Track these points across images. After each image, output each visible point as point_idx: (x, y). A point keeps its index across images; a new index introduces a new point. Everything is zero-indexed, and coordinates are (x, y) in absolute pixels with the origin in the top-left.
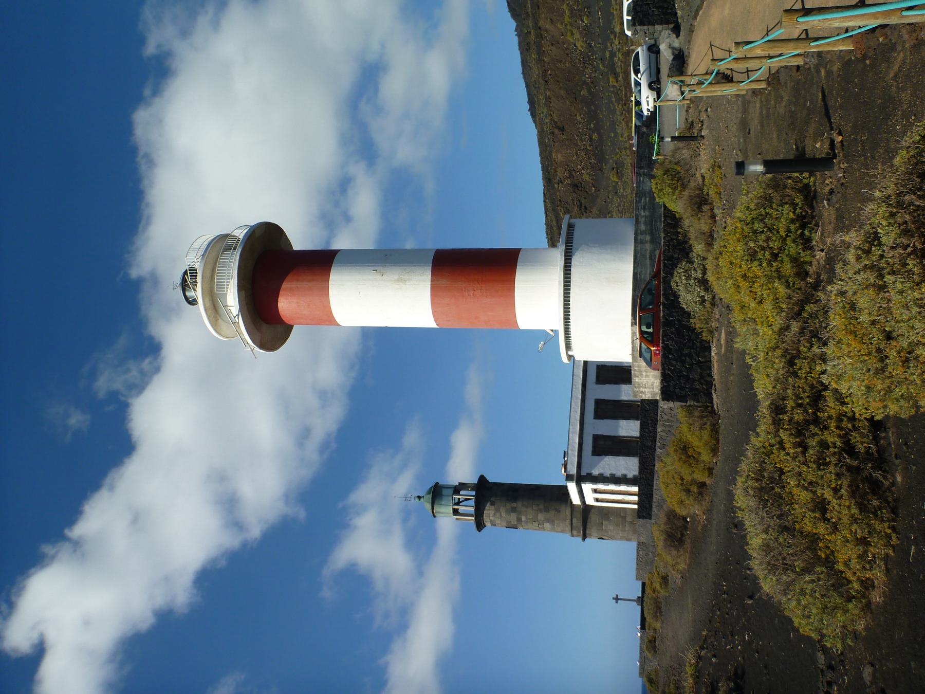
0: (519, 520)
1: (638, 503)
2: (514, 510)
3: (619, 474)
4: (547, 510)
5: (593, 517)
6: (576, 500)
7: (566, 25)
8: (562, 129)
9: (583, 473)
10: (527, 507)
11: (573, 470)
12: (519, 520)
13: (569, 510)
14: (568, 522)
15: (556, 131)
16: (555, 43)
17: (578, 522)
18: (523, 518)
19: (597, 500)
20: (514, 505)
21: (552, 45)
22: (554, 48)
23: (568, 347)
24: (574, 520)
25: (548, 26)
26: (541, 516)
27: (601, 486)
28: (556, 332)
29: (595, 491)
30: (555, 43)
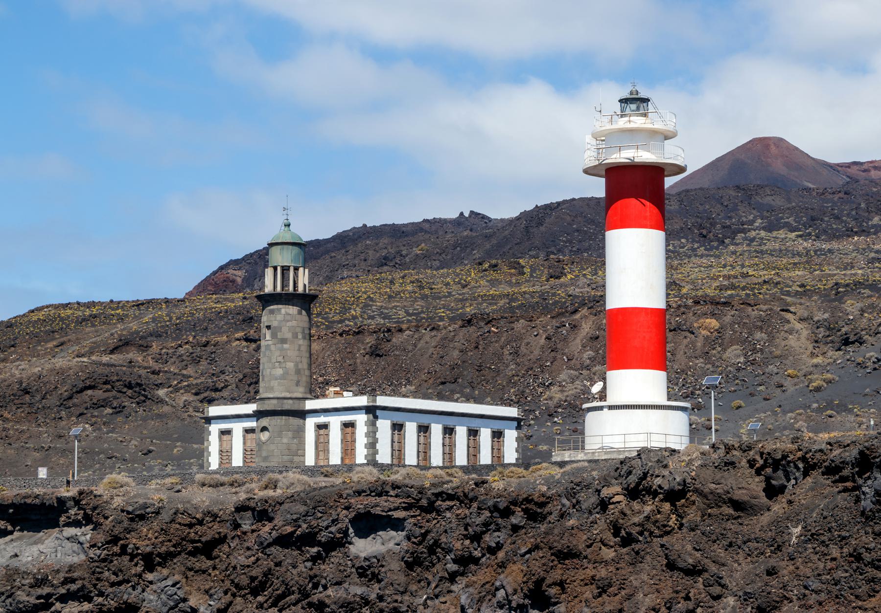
0: (284, 341)
2: (295, 336)
3: (378, 446)
4: (298, 372)
5: (294, 421)
7: (588, 368)
8: (375, 353)
9: (378, 412)
10: (299, 350)
11: (382, 401)
12: (284, 341)
13: (300, 396)
14: (288, 395)
15: (370, 340)
16: (553, 345)
17: (288, 405)
18: (285, 346)
20: (300, 336)
21: (548, 338)
22: (542, 341)
23: (611, 408)
24: (290, 401)
26: (290, 365)
28: (602, 395)
30: (553, 345)
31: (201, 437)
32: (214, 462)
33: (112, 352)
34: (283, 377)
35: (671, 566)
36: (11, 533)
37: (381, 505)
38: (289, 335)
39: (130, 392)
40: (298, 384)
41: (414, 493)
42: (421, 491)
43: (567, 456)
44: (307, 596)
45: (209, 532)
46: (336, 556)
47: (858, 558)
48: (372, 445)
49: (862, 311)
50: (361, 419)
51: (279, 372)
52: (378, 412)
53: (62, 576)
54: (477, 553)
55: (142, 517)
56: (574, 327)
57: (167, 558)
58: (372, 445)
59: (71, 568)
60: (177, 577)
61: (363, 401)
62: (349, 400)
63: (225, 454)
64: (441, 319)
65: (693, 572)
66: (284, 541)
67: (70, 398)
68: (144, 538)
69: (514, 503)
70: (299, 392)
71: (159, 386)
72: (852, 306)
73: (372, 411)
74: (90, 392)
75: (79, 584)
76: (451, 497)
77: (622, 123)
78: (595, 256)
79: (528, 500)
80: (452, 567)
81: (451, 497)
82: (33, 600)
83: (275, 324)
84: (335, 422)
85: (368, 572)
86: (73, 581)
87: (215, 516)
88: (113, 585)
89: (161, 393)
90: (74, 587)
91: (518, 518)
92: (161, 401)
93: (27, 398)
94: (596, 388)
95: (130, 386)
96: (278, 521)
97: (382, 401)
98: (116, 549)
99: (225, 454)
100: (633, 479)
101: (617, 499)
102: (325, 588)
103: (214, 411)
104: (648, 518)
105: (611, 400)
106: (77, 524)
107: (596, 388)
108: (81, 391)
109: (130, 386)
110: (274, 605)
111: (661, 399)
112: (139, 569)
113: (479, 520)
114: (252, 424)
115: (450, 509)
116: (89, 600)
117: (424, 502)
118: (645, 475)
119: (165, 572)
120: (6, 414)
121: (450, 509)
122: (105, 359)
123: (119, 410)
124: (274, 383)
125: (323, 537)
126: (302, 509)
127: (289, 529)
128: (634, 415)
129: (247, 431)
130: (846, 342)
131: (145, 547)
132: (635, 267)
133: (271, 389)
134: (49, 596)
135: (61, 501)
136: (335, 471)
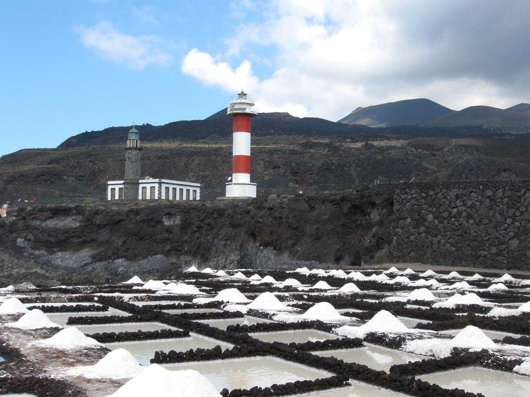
0: (133, 162)
1: (143, 200)
2: (136, 160)
4: (137, 171)
6: (140, 181)
7: (197, 173)
9: (162, 184)
12: (133, 162)
17: (134, 181)
19: (144, 188)
21: (185, 164)
25: (196, 161)
26: (135, 169)
27: (157, 189)
28: (231, 181)
29: (153, 188)
31: (106, 189)
32: (109, 198)
33: (48, 164)
34: (133, 172)
35: (290, 226)
36: (54, 218)
37: (173, 211)
38: (134, 160)
39: (55, 177)
40: (137, 175)
41: (183, 208)
42: (185, 207)
43: (221, 198)
44: (151, 237)
45: (117, 218)
46: (159, 226)
47: (344, 225)
48: (160, 194)
49: (279, 158)
50: (157, 186)
51: (131, 171)
52: (162, 184)
53: (72, 231)
54: (202, 225)
55: (97, 213)
56: (193, 161)
57: (105, 226)
58: (160, 194)
59: (75, 228)
60: (108, 231)
61: (157, 180)
62: (151, 180)
63: (113, 195)
64: (151, 157)
65: (296, 229)
66: (143, 221)
67: (36, 178)
68: (98, 220)
69: (215, 211)
70: (137, 177)
71: (64, 175)
72: (276, 157)
73: (160, 183)
74: (42, 177)
75: (78, 233)
76: (195, 209)
77: (239, 101)
78: (230, 140)
79: (219, 210)
80: (195, 229)
81: (195, 209)
82: (63, 238)
83: (130, 157)
84: (148, 186)
85: (169, 230)
86: (76, 232)
87: (120, 213)
88: (88, 233)
89: (65, 177)
90: (76, 234)
91: (215, 215)
92: (65, 180)
93: (23, 178)
94: (229, 179)
95: (55, 175)
96: (142, 215)
97: (163, 180)
98: (89, 223)
99: (113, 195)
100: (258, 204)
101: (253, 210)
102: (157, 234)
103: (109, 182)
104: (263, 215)
105: (234, 182)
106: (76, 215)
107: (229, 179)
108: (39, 176)
109: (55, 175)
110: (141, 239)
111: (249, 182)
112: (97, 229)
113: (204, 216)
114: (122, 186)
115: (193, 212)
116: (81, 238)
117: (186, 210)
118: (262, 203)
119: (104, 230)
120: (16, 183)
121: (193, 212)
122: (46, 166)
123: (52, 182)
124: (130, 175)
125: (156, 220)
126: (149, 212)
127: (145, 218)
128: (241, 187)
129: (120, 189)
130: (275, 168)
131: (98, 222)
132: (242, 143)
133: (129, 176)
134: (68, 236)
135: (70, 208)
136: (148, 201)
